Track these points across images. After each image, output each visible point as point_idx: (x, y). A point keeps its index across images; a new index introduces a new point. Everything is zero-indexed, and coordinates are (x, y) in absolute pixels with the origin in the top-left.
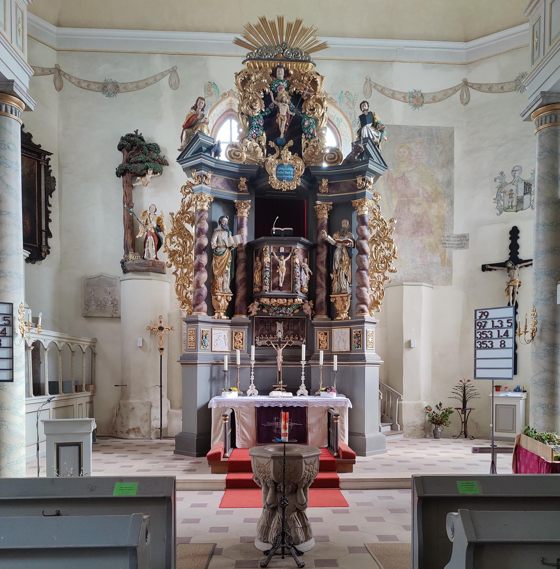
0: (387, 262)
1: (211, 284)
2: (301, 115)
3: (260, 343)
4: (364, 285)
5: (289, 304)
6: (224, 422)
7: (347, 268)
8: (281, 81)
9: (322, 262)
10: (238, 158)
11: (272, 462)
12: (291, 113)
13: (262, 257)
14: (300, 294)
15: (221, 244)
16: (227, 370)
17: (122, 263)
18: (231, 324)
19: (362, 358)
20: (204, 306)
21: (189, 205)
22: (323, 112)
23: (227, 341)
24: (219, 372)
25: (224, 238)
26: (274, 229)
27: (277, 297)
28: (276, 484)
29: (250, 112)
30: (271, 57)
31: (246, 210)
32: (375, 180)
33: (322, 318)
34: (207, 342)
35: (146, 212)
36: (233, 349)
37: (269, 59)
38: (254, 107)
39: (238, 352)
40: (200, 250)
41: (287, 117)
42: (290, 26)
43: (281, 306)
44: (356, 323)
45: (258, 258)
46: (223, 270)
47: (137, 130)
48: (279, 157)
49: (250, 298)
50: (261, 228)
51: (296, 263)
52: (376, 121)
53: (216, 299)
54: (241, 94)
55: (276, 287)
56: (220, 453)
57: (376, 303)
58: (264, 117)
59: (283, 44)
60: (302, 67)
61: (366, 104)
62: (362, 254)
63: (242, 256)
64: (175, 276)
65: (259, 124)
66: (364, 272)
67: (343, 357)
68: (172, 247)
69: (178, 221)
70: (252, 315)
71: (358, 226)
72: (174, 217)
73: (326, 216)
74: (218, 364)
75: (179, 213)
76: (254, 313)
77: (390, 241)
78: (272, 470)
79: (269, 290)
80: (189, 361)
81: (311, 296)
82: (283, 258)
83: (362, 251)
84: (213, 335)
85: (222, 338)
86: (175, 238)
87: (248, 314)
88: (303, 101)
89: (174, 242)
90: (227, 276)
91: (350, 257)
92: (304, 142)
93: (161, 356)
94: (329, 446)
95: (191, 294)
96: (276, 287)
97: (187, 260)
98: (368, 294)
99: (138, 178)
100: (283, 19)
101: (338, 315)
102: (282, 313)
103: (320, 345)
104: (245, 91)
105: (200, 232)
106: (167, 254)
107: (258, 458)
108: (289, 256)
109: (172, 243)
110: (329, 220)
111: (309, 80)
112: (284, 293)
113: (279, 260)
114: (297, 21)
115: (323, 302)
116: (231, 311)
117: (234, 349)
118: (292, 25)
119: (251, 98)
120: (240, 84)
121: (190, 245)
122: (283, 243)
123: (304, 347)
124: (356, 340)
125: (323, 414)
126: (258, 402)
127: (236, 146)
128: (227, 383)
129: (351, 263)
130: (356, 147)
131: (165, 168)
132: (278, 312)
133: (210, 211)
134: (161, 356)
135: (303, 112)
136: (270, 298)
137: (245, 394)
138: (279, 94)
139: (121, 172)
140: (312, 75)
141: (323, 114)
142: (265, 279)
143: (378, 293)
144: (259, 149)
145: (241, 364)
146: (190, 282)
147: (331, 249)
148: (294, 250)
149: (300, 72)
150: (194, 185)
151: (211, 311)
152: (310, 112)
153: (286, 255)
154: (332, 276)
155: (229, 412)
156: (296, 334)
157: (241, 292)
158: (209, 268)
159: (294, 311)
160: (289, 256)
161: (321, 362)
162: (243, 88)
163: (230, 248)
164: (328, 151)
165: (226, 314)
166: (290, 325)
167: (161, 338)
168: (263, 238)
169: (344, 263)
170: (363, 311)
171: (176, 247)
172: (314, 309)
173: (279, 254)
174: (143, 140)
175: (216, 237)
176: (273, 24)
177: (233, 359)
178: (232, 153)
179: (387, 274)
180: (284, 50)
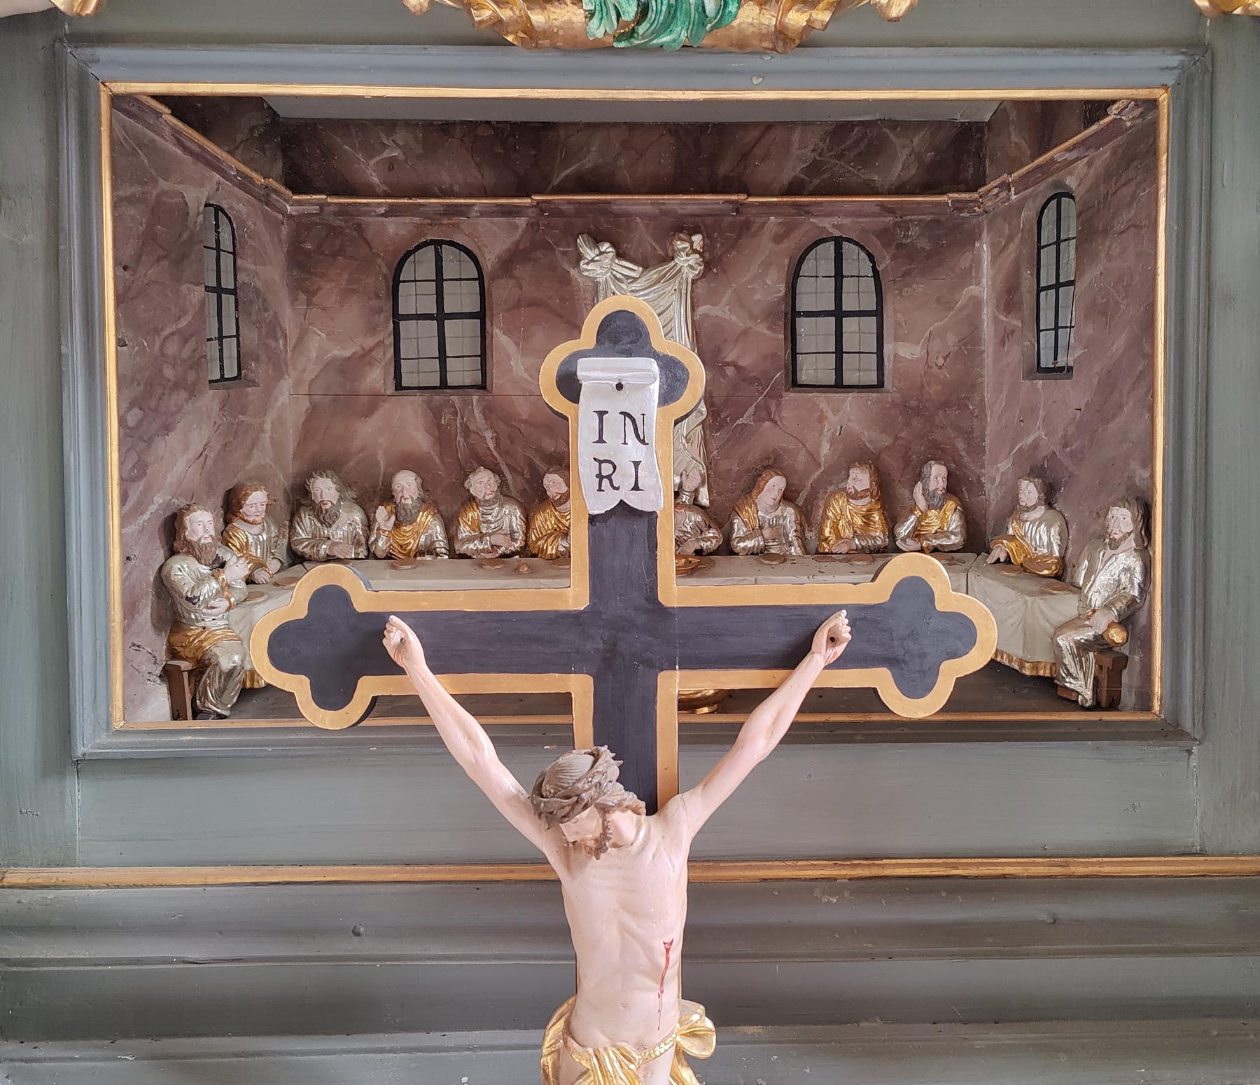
166: (815, 293)
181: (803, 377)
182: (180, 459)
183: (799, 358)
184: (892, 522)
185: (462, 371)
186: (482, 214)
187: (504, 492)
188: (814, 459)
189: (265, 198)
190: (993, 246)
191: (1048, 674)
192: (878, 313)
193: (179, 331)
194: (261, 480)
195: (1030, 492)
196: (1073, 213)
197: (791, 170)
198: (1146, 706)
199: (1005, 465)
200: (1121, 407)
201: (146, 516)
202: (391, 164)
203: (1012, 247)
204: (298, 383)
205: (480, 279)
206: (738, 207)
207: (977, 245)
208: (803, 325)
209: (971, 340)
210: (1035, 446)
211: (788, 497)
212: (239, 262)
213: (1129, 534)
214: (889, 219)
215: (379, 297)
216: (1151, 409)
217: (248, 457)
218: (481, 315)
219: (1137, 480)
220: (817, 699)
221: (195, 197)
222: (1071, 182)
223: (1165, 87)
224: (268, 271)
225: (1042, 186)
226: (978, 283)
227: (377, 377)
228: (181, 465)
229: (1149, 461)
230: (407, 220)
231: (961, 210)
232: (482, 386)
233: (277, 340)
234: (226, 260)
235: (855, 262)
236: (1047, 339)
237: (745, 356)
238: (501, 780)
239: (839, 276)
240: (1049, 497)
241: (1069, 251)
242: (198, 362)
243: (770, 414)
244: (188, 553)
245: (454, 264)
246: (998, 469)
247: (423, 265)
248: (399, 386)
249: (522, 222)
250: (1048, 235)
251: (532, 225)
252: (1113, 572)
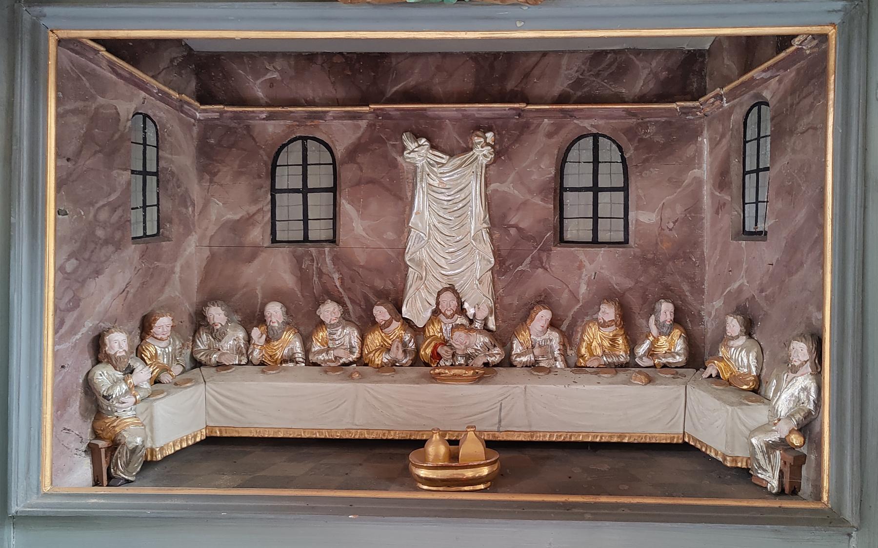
3: (169, 420)
166: (578, 174)
181: (569, 236)
182: (105, 294)
183: (566, 221)
184: (632, 344)
185: (319, 230)
186: (335, 118)
188: (574, 295)
189: (180, 107)
190: (711, 140)
191: (744, 466)
192: (625, 189)
193: (109, 204)
194: (169, 308)
195: (734, 326)
196: (769, 117)
197: (560, 86)
198: (818, 498)
199: (718, 304)
200: (802, 264)
201: (78, 337)
202: (272, 83)
203: (724, 141)
204: (201, 239)
205: (334, 164)
206: (520, 113)
207: (700, 139)
208: (569, 197)
209: (694, 210)
210: (740, 290)
211: (554, 324)
212: (160, 153)
213: (806, 362)
214: (633, 121)
215: (259, 177)
216: (822, 266)
217: (161, 291)
218: (333, 190)
219: (813, 320)
221: (126, 108)
222: (767, 95)
223: (833, 24)
224: (183, 159)
225: (746, 97)
226: (700, 168)
227: (258, 234)
228: (107, 299)
229: (821, 308)
230: (282, 122)
231: (686, 114)
232: (333, 241)
233: (187, 208)
234: (151, 152)
235: (609, 152)
236: (750, 210)
237: (524, 220)
239: (596, 162)
240: (749, 328)
241: (766, 144)
242: (124, 225)
243: (542, 263)
244: (108, 362)
245: (315, 153)
246: (713, 306)
247: (294, 154)
248: (274, 241)
249: (363, 123)
250: (751, 133)
251: (371, 126)
252: (792, 392)
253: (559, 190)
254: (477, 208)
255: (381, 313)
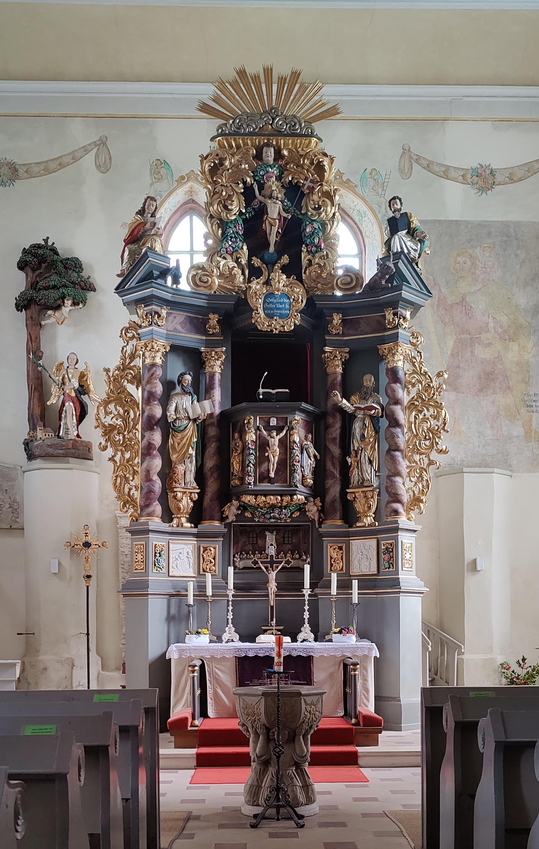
0: (434, 438)
1: (168, 474)
2: (300, 216)
3: (241, 564)
4: (398, 474)
5: (284, 504)
6: (191, 675)
7: (371, 447)
8: (270, 166)
9: (334, 439)
10: (206, 285)
11: (263, 700)
12: (285, 215)
13: (242, 433)
14: (301, 488)
15: (182, 415)
16: (192, 603)
17: (27, 444)
18: (197, 535)
19: (396, 583)
20: (157, 508)
21: (133, 357)
22: (333, 211)
23: (191, 561)
24: (179, 607)
25: (186, 407)
26: (261, 390)
27: (266, 494)
28: (268, 730)
29: (223, 215)
30: (254, 129)
31: (219, 363)
32: (413, 315)
33: (335, 523)
34: (163, 562)
35: (62, 364)
36: (201, 573)
37: (251, 134)
38: (230, 207)
39: (209, 576)
40: (150, 424)
41: (280, 220)
42: (282, 81)
43: (273, 507)
44: (386, 531)
45: (236, 435)
46: (185, 453)
47: (48, 238)
48: (267, 283)
49: (226, 494)
50: (242, 389)
51: (295, 442)
52: (413, 226)
53: (175, 497)
54: (210, 187)
55: (265, 478)
56: (186, 719)
57: (416, 501)
58: (244, 221)
59: (272, 109)
60: (300, 144)
61: (398, 201)
62: (394, 427)
63: (212, 432)
64: (111, 464)
65: (237, 233)
66: (398, 454)
67: (367, 583)
68: (108, 421)
69: (116, 382)
70: (228, 521)
71: (389, 383)
72: (111, 374)
73: (340, 370)
74: (178, 595)
75: (118, 369)
76: (232, 518)
77: (438, 406)
78: (262, 711)
79: (255, 482)
80: (135, 590)
81: (318, 490)
82: (274, 434)
83: (395, 423)
84: (171, 552)
85: (184, 556)
86: (111, 407)
87: (222, 519)
88: (303, 195)
89: (111, 413)
90: (191, 462)
91: (377, 432)
92: (305, 257)
93: (88, 587)
94: (346, 714)
95: (137, 490)
96: (264, 477)
97: (130, 440)
98: (405, 487)
99: (50, 312)
100: (272, 69)
101: (358, 519)
102: (274, 518)
103: (332, 565)
104: (215, 183)
105: (149, 398)
106: (100, 431)
107: (245, 698)
108: (284, 432)
109: (107, 413)
110: (343, 375)
111: (312, 163)
112: (276, 487)
113: (268, 438)
114: (293, 73)
115: (337, 499)
116: (197, 516)
117: (202, 572)
118: (285, 79)
119: (224, 193)
120: (207, 173)
121: (135, 415)
122: (274, 412)
123: (307, 568)
124: (386, 557)
125: (337, 667)
126: (240, 649)
127: (203, 269)
128: (193, 623)
129: (377, 439)
130: (382, 264)
131: (90, 295)
132: (268, 516)
133: (164, 366)
134: (88, 587)
135: (303, 212)
136: (256, 495)
137: (219, 639)
138: (266, 186)
139: (23, 304)
140: (316, 156)
141: (334, 214)
142: (248, 466)
143: (420, 486)
144: (237, 271)
145: (212, 596)
146: (135, 473)
147: (348, 419)
148: (291, 422)
149: (298, 152)
150: (140, 327)
151: (168, 515)
152: (314, 212)
153: (279, 429)
154: (349, 460)
155: (198, 663)
156: (297, 550)
157: (212, 487)
158: (164, 451)
159: (292, 514)
160: (284, 432)
161: (334, 590)
162: (212, 179)
163: (195, 420)
164: (340, 272)
165: (189, 520)
167: (87, 559)
168: (244, 404)
169: (367, 440)
170: (396, 512)
171: (114, 419)
172: (321, 510)
173: (269, 429)
174: (56, 253)
175: (174, 405)
176: (256, 79)
177: (201, 588)
178: (197, 278)
179: (434, 455)
180: (273, 119)
187: (259, 553)
218: (257, 537)
220: (282, 567)
227: (247, 543)
232: (257, 543)
235: (290, 533)
238: (265, 570)
247: (252, 533)
253: (284, 538)
254: (274, 540)
255: (263, 552)
